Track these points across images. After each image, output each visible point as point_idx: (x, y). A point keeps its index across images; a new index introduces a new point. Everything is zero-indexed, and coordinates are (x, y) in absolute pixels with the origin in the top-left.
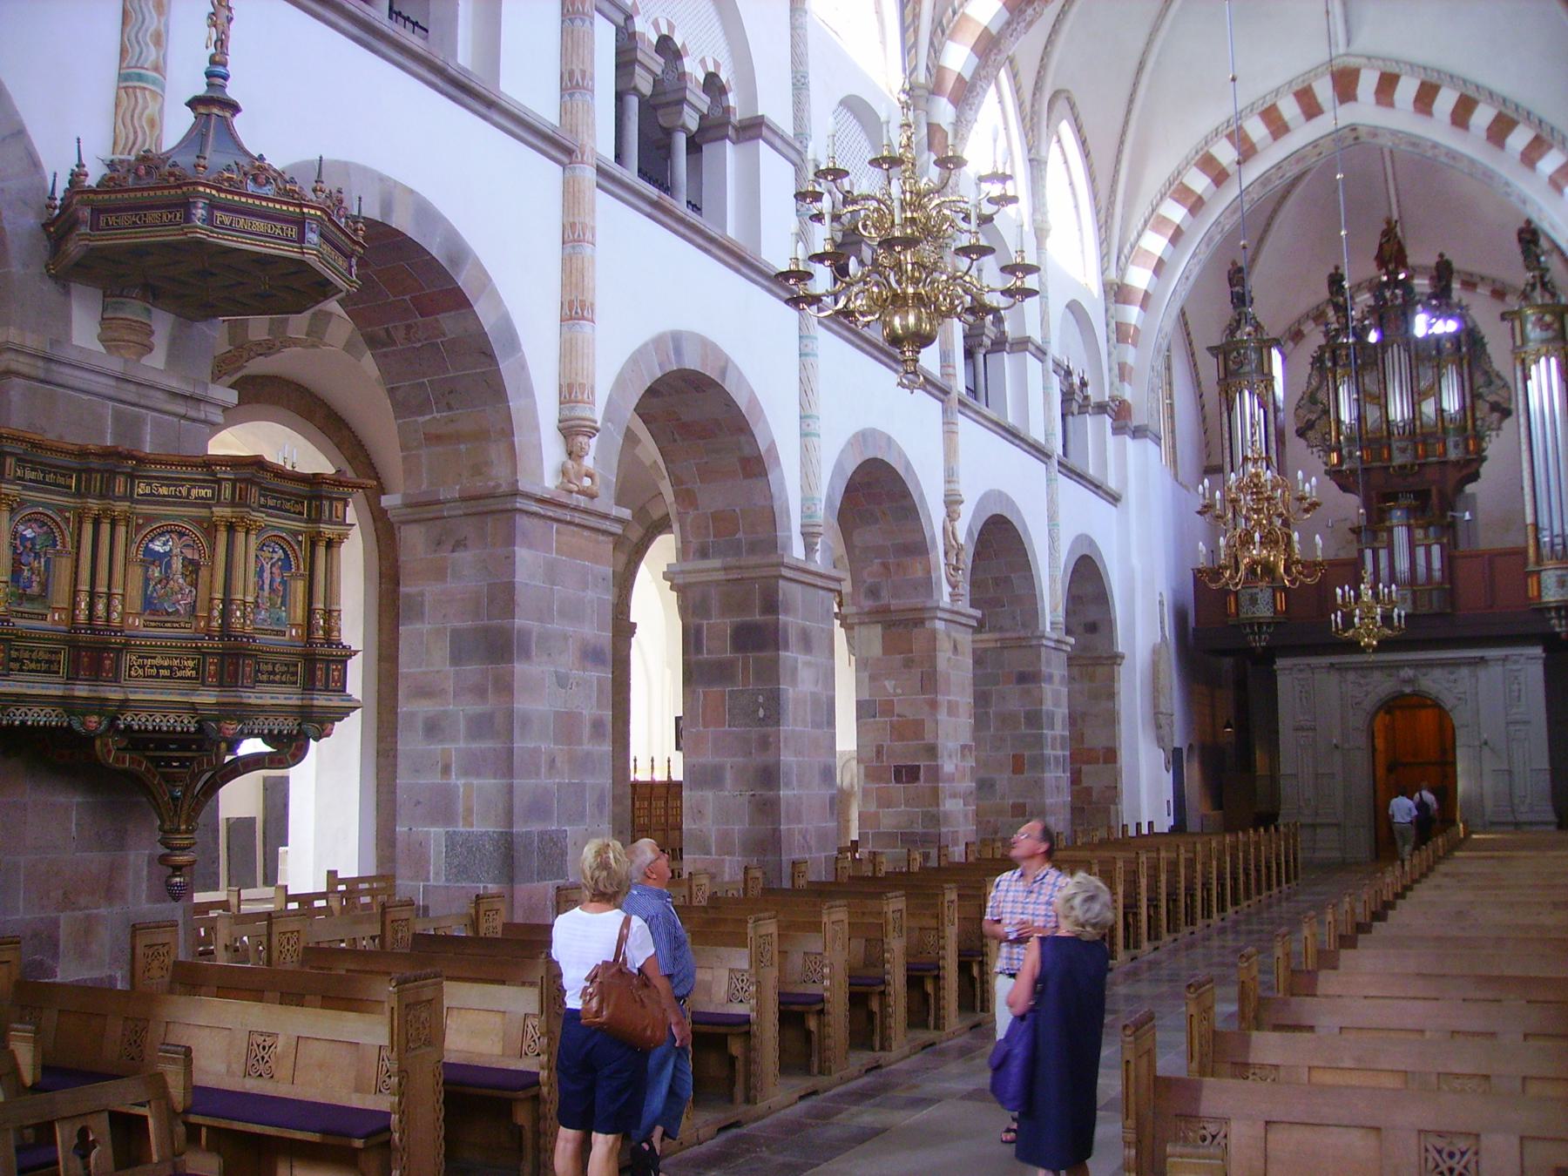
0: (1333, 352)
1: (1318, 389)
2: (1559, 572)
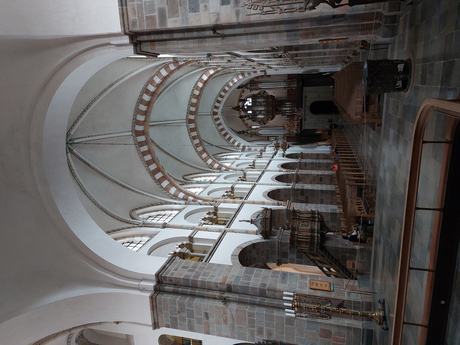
0: (252, 118)
1: (258, 121)
2: (292, 84)
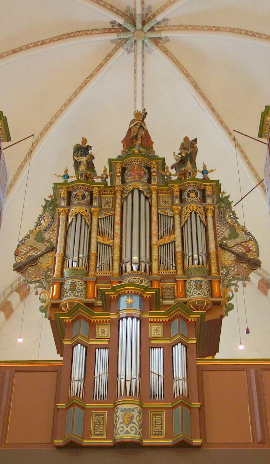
0: (69, 193)
